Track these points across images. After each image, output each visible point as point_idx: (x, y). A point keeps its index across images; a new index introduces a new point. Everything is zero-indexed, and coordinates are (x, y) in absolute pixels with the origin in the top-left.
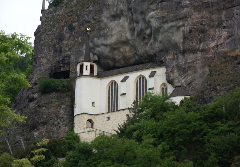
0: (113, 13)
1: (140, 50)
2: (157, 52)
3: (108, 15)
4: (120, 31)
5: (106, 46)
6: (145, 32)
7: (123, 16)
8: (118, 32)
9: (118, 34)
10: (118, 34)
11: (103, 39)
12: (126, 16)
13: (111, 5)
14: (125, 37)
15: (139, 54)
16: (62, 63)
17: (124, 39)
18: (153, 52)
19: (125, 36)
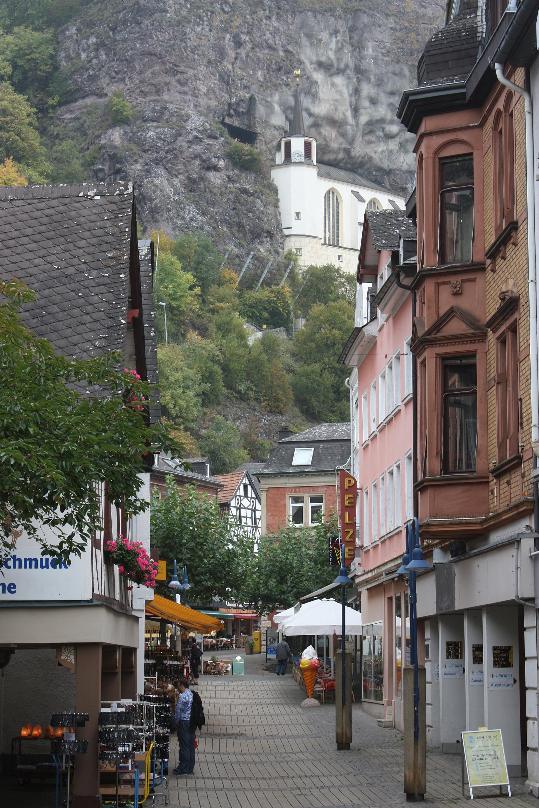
0: (323, 59)
1: (358, 149)
2: (400, 170)
3: (314, 59)
4: (336, 101)
5: (310, 114)
6: (384, 126)
7: (343, 75)
8: (333, 100)
9: (332, 102)
10: (332, 102)
11: (310, 100)
12: (349, 78)
13: (324, 43)
14: (341, 115)
15: (353, 154)
16: (234, 110)
17: (338, 116)
18: (388, 165)
19: (344, 114)
